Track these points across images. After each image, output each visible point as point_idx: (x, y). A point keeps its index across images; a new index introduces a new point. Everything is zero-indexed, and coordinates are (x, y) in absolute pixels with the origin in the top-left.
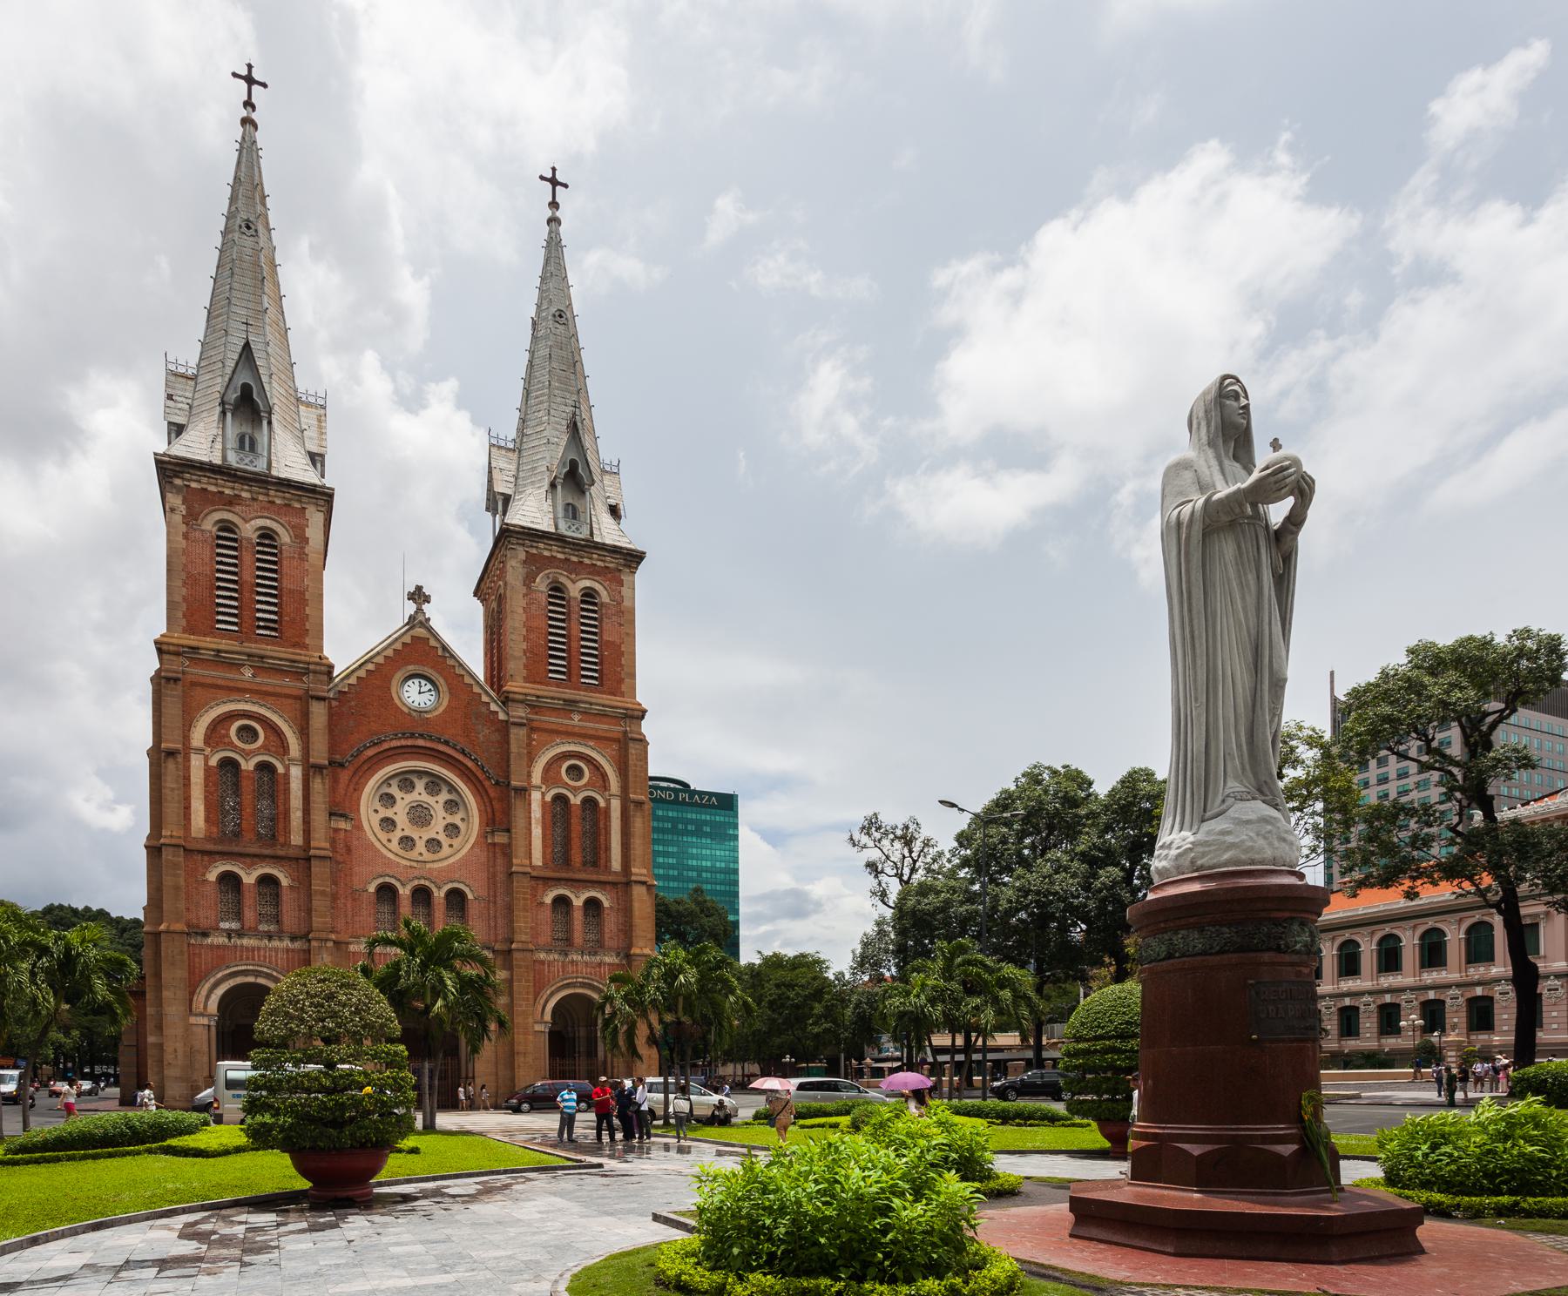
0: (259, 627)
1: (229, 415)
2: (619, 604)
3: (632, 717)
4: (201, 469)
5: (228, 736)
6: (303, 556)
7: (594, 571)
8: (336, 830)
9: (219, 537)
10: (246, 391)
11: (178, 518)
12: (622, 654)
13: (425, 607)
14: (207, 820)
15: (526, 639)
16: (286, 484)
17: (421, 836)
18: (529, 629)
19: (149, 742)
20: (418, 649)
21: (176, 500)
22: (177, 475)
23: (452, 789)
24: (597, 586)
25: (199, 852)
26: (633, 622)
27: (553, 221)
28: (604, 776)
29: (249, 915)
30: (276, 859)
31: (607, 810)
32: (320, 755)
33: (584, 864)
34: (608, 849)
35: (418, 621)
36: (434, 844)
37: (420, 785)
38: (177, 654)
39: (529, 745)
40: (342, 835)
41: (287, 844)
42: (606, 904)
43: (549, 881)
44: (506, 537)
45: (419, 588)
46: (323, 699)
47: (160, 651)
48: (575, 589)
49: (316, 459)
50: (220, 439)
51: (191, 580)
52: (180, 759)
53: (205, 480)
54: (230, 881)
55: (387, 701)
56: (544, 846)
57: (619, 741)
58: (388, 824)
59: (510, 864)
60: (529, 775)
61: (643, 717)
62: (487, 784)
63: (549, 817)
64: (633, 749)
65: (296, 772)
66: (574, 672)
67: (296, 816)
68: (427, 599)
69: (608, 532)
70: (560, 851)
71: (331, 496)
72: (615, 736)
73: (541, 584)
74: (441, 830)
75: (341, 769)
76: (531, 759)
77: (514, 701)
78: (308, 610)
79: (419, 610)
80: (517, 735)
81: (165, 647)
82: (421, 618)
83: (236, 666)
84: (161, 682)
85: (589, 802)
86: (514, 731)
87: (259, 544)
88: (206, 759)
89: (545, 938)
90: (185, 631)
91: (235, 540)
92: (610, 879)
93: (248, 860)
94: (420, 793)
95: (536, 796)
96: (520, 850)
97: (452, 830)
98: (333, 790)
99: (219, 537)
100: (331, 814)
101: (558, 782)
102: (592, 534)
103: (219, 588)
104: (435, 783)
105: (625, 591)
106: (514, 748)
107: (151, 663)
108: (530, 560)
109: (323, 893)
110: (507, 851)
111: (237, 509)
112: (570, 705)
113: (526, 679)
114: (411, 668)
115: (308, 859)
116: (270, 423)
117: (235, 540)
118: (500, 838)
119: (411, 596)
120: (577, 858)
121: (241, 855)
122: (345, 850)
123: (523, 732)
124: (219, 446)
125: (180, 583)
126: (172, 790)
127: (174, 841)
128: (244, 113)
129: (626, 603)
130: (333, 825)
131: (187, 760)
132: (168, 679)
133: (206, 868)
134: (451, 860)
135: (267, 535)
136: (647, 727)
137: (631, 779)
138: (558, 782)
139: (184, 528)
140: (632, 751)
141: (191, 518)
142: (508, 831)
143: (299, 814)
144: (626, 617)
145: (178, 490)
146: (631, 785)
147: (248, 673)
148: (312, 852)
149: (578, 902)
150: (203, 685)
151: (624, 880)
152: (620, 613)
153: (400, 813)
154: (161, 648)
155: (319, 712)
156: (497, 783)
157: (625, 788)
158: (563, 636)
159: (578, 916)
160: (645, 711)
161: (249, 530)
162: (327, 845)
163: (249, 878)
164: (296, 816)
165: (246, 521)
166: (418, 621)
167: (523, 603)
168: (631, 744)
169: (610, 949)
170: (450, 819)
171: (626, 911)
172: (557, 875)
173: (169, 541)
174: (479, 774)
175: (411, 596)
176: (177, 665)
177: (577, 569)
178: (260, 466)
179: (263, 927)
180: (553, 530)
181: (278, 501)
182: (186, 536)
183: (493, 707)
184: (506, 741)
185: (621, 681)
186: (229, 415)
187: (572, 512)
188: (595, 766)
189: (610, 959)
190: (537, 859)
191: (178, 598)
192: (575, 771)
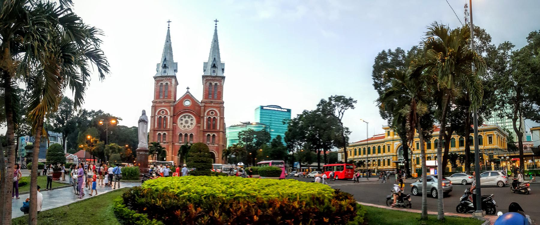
6: (171, 86)
7: (217, 80)
17: (187, 125)
20: (188, 96)
32: (172, 115)
35: (188, 92)
36: (188, 126)
37: (187, 117)
48: (213, 84)
51: (157, 92)
55: (182, 105)
58: (182, 124)
65: (169, 117)
69: (220, 74)
70: (208, 126)
75: (175, 116)
80: (203, 108)
84: (152, 107)
94: (187, 119)
97: (192, 124)
98: (173, 119)
104: (189, 117)
107: (152, 104)
108: (207, 80)
112: (212, 102)
118: (199, 125)
122: (174, 129)
135: (167, 84)
136: (224, 105)
141: (157, 83)
144: (222, 87)
153: (183, 122)
155: (172, 108)
161: (164, 84)
163: (162, 134)
166: (188, 92)
176: (154, 104)
177: (213, 80)
178: (166, 74)
184: (200, 109)
187: (214, 72)
190: (205, 128)
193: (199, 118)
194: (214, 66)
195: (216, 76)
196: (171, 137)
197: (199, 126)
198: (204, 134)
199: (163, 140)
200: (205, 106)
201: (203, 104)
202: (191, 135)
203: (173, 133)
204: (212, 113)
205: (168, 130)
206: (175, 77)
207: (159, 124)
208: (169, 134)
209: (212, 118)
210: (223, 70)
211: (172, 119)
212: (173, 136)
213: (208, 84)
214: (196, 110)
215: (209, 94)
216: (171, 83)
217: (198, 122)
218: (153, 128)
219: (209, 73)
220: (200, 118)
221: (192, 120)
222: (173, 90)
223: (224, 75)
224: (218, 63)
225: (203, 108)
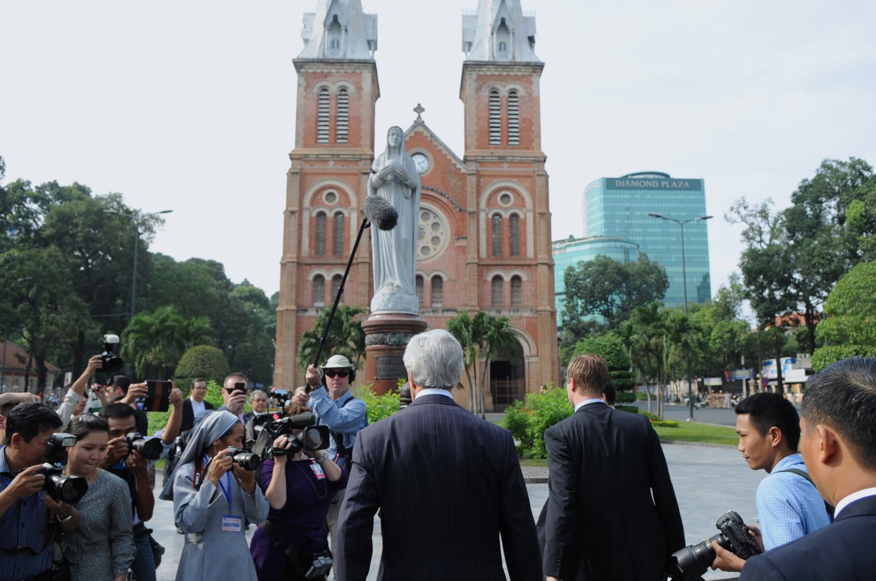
2: (530, 95)
3: (538, 161)
6: (360, 98)
7: (516, 78)
10: (335, 18)
11: (302, 89)
12: (533, 124)
13: (422, 115)
14: (310, 246)
15: (477, 124)
16: (352, 62)
18: (479, 118)
21: (302, 80)
22: (301, 67)
23: (436, 216)
24: (517, 87)
26: (538, 105)
28: (523, 199)
33: (512, 254)
34: (525, 244)
35: (419, 123)
38: (299, 159)
39: (478, 185)
44: (467, 66)
45: (419, 105)
47: (291, 159)
48: (504, 92)
52: (297, 215)
54: (319, 278)
56: (488, 245)
57: (530, 177)
60: (478, 203)
61: (545, 161)
62: (454, 211)
63: (490, 227)
64: (539, 181)
68: (423, 110)
69: (524, 56)
71: (374, 64)
73: (486, 93)
74: (429, 240)
76: (479, 193)
78: (362, 126)
79: (419, 117)
82: (419, 121)
83: (325, 161)
84: (292, 174)
85: (514, 216)
86: (469, 178)
88: (311, 213)
92: (527, 262)
93: (328, 267)
95: (483, 215)
97: (435, 239)
101: (496, 205)
102: (514, 58)
105: (534, 87)
107: (288, 164)
108: (479, 78)
109: (364, 283)
111: (329, 79)
112: (502, 158)
113: (478, 147)
114: (414, 150)
116: (346, 31)
118: (463, 243)
119: (415, 110)
123: (474, 178)
129: (535, 94)
132: (293, 173)
133: (308, 273)
134: (435, 258)
136: (548, 167)
138: (496, 205)
139: (304, 93)
144: (534, 102)
145: (303, 74)
147: (331, 164)
151: (535, 263)
152: (532, 100)
154: (292, 157)
156: (460, 210)
157: (534, 206)
159: (507, 287)
160: (545, 157)
161: (333, 89)
163: (328, 277)
165: (334, 84)
166: (419, 123)
170: (435, 234)
171: (535, 282)
174: (450, 206)
175: (415, 110)
178: (340, 55)
180: (491, 59)
181: (349, 71)
182: (305, 98)
183: (458, 166)
184: (464, 185)
185: (532, 140)
187: (502, 47)
189: (527, 314)
193: (461, 215)
194: (502, 26)
195: (513, 65)
197: (463, 249)
200: (479, 175)
201: (473, 167)
202: (437, 279)
207: (317, 239)
209: (506, 215)
210: (531, 40)
214: (449, 187)
215: (490, 130)
216: (359, 88)
217: (459, 234)
219: (484, 52)
220: (463, 219)
221: (435, 225)
222: (365, 114)
223: (540, 53)
225: (471, 181)
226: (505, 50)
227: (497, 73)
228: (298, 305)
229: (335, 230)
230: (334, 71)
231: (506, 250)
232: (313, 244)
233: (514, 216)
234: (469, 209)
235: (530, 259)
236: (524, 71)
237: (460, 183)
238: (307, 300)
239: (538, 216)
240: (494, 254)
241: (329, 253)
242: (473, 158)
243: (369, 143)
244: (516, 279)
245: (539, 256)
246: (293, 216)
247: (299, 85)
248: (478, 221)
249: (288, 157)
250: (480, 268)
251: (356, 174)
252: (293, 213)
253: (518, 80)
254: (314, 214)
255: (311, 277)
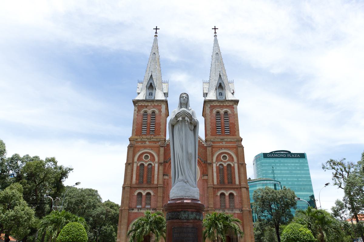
0: (151, 132)
1: (147, 89)
3: (239, 141)
4: (141, 101)
5: (142, 158)
6: (160, 115)
7: (227, 107)
8: (165, 179)
9: (144, 114)
10: (151, 85)
11: (136, 112)
12: (235, 125)
14: (136, 179)
15: (211, 125)
19: (126, 162)
21: (136, 108)
24: (228, 110)
25: (134, 187)
27: (216, 36)
28: (232, 158)
29: (143, 203)
30: (151, 188)
31: (234, 167)
32: (162, 160)
33: (229, 183)
34: (235, 178)
39: (212, 152)
40: (166, 180)
41: (153, 184)
42: (235, 194)
43: (219, 189)
44: (205, 102)
46: (163, 147)
49: (166, 94)
50: (145, 94)
51: (137, 124)
52: (131, 165)
53: (142, 103)
54: (140, 194)
56: (217, 178)
57: (236, 148)
59: (208, 185)
60: (212, 160)
61: (242, 141)
62: (202, 163)
63: (218, 171)
64: (239, 149)
65: (156, 165)
66: (223, 131)
67: (156, 176)
69: (230, 97)
71: (167, 102)
72: (235, 146)
76: (212, 155)
77: (208, 141)
78: (161, 127)
80: (209, 149)
81: (131, 140)
84: (130, 147)
85: (229, 165)
86: (208, 148)
87: (152, 114)
88: (137, 164)
89: (218, 206)
90: (135, 135)
91: (147, 114)
92: (236, 187)
93: (144, 189)
95: (214, 165)
96: (210, 181)
98: (164, 169)
99: (144, 114)
100: (164, 175)
102: (226, 98)
103: (143, 125)
105: (235, 110)
106: (208, 153)
109: (160, 196)
110: (206, 181)
111: (148, 108)
113: (212, 135)
115: (158, 187)
116: (155, 89)
117: (147, 114)
118: (206, 177)
120: (226, 181)
121: (143, 188)
124: (145, 96)
125: (135, 125)
126: (129, 172)
127: (128, 185)
128: (155, 34)
129: (235, 113)
130: (164, 178)
131: (133, 165)
132: (130, 147)
133: (135, 191)
136: (243, 143)
137: (239, 158)
139: (137, 113)
140: (239, 150)
141: (139, 111)
142: (207, 175)
143: (157, 176)
144: (235, 116)
146: (239, 159)
147: (147, 143)
148: (158, 186)
149: (227, 194)
150: (138, 147)
151: (240, 187)
152: (234, 115)
155: (162, 150)
158: (220, 123)
159: (227, 199)
160: (242, 139)
161: (150, 112)
162: (162, 183)
163: (144, 194)
164: (156, 176)
167: (210, 117)
168: (239, 148)
169: (237, 208)
171: (241, 196)
172: (221, 187)
173: (134, 117)
179: (147, 207)
180: (216, 99)
181: (156, 105)
182: (137, 115)
183: (203, 143)
186: (147, 89)
187: (221, 94)
188: (230, 155)
189: (237, 212)
190: (215, 182)
191: (134, 128)
192: (225, 157)
196: (160, 199)
198: (215, 193)
199: (146, 204)
203: (164, 193)
204: (225, 157)
205: (156, 188)
206: (166, 102)
207: (140, 176)
208: (156, 193)
209: (225, 165)
211: (161, 168)
212: (163, 197)
213: (214, 112)
215: (217, 127)
216: (160, 111)
218: (128, 182)
219: (212, 96)
220: (206, 167)
224: (225, 82)
226: (222, 95)
227: (218, 105)
228: (129, 207)
229: (148, 172)
230: (150, 104)
231: (226, 181)
232: (138, 178)
233: (229, 165)
234: (209, 162)
235: (237, 185)
236: (231, 104)
237: (204, 151)
238: (133, 204)
239: (240, 165)
240: (221, 183)
241: (145, 182)
242: (210, 140)
243: (164, 134)
244: (231, 195)
245: (242, 184)
246: (129, 166)
247: (135, 110)
248: (213, 167)
249: (129, 140)
250: (214, 190)
251: (158, 147)
252: (129, 164)
253: (228, 107)
254: (139, 165)
255: (136, 194)
